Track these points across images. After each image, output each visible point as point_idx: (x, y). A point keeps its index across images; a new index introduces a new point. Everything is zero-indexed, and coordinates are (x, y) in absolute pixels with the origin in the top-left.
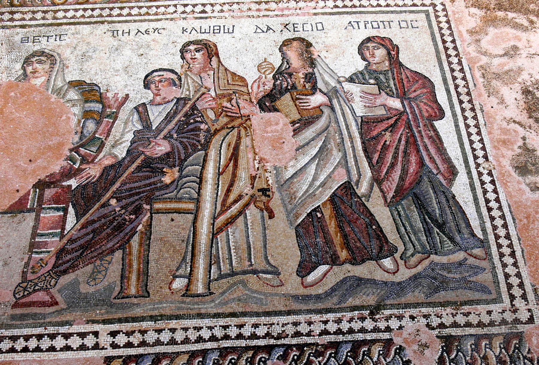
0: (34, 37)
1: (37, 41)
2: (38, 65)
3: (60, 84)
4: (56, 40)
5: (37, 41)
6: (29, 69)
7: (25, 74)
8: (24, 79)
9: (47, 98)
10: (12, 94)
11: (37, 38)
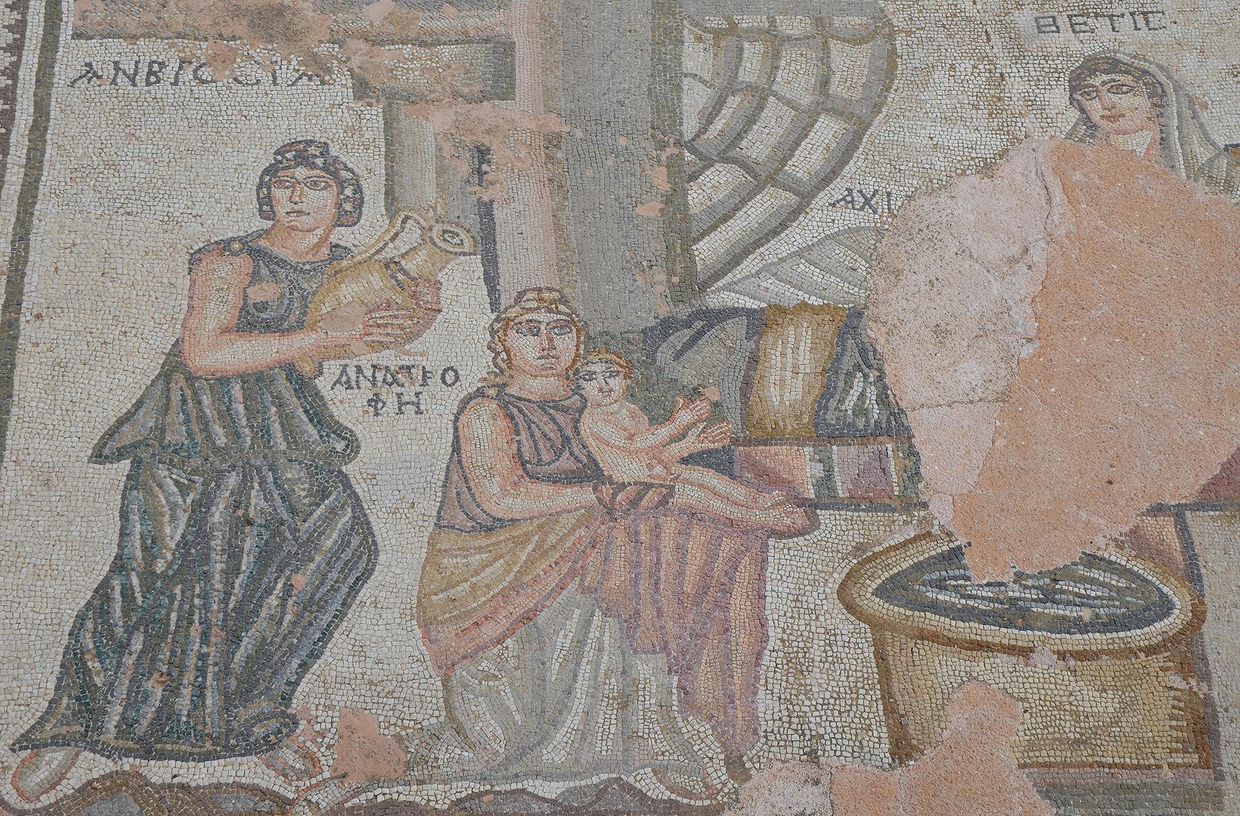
0: (1070, 17)
1: (1083, 28)
2: (1115, 98)
3: (1203, 154)
4: (1136, 28)
5: (1083, 28)
6: (1096, 109)
7: (1086, 118)
8: (1092, 136)
9: (1181, 192)
10: (1078, 176)
11: (1080, 20)
